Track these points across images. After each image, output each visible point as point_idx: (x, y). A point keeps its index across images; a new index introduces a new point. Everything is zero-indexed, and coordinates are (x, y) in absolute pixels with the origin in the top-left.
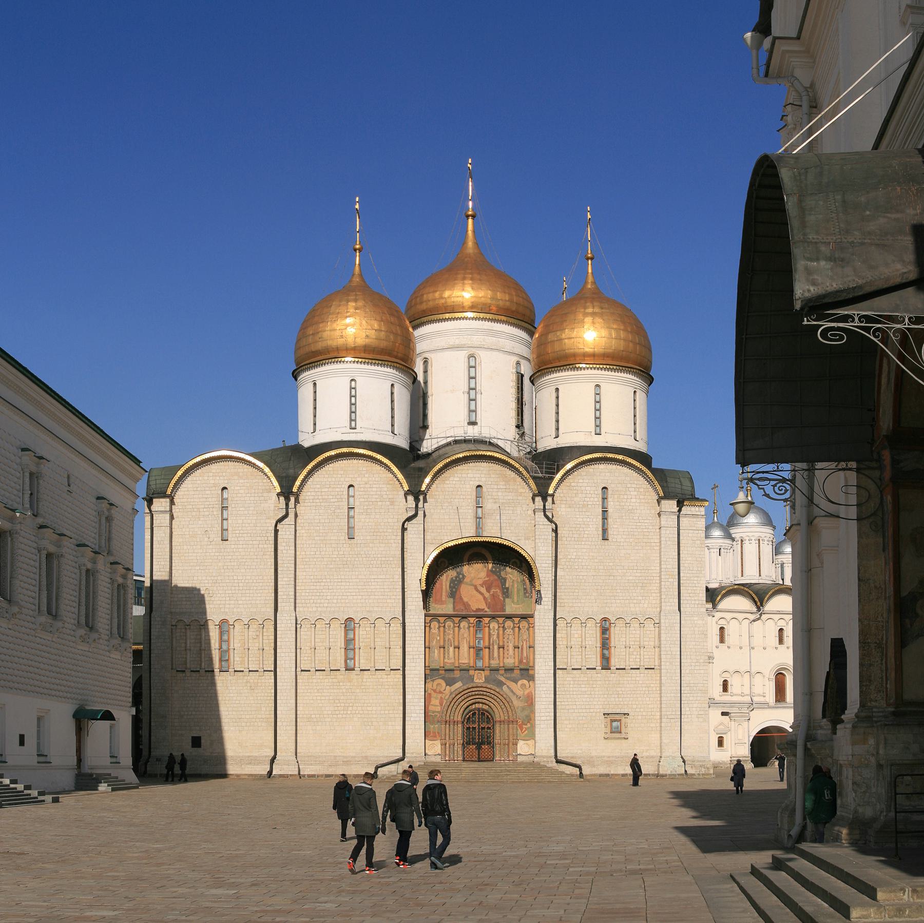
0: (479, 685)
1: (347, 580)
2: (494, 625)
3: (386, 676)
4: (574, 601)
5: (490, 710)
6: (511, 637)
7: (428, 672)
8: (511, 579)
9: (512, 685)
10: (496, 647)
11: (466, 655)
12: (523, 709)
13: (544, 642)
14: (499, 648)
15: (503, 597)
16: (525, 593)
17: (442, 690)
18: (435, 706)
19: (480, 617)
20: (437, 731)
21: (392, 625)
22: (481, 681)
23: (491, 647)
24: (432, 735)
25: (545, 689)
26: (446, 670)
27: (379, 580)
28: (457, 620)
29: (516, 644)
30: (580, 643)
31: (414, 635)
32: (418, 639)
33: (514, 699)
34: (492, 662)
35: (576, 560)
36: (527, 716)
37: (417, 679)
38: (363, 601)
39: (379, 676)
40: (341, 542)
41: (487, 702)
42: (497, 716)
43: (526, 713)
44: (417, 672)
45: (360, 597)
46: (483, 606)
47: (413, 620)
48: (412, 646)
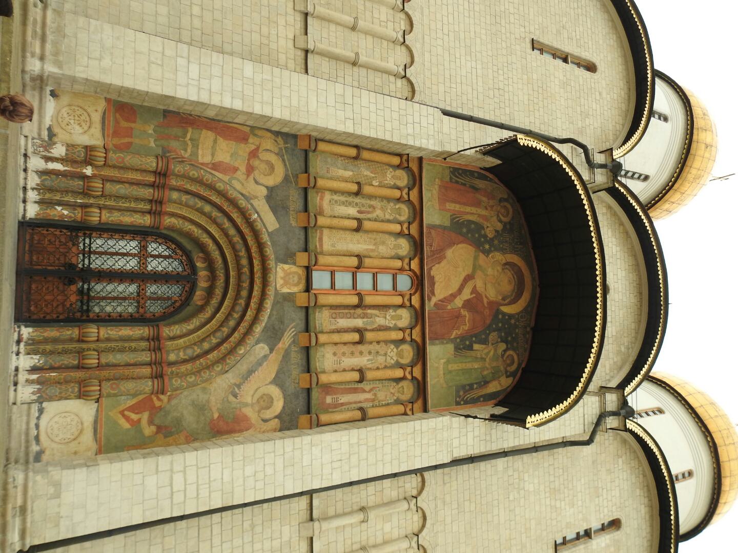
0: (271, 278)
1: (472, 13)
2: (405, 318)
3: (291, 36)
4: (455, 506)
5: (189, 310)
6: (381, 359)
7: (303, 145)
8: (487, 354)
9: (269, 370)
10: (359, 323)
11: (342, 246)
12: (201, 408)
13: (387, 448)
14: (358, 330)
15: (456, 338)
16: (463, 387)
17: (256, 172)
18: (214, 148)
19: (420, 282)
20: (136, 141)
21: (399, 82)
22: (280, 282)
23: (359, 311)
24: (124, 124)
25: (269, 470)
26: (305, 190)
27: (474, 77)
28: (414, 230)
29: (369, 375)
30: (371, 542)
31: (395, 115)
32: (388, 126)
33: (231, 378)
34: (326, 313)
35: (522, 492)
36: (178, 422)
37: (295, 103)
38: (440, 35)
39: (291, 19)
40: (527, 24)
41: (215, 302)
42: (176, 330)
43: (190, 419)
44: (313, 106)
45: (446, 31)
46: (441, 292)
47: (424, 124)
48: (373, 107)
